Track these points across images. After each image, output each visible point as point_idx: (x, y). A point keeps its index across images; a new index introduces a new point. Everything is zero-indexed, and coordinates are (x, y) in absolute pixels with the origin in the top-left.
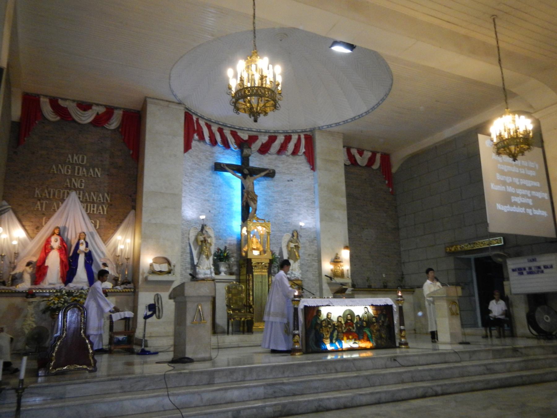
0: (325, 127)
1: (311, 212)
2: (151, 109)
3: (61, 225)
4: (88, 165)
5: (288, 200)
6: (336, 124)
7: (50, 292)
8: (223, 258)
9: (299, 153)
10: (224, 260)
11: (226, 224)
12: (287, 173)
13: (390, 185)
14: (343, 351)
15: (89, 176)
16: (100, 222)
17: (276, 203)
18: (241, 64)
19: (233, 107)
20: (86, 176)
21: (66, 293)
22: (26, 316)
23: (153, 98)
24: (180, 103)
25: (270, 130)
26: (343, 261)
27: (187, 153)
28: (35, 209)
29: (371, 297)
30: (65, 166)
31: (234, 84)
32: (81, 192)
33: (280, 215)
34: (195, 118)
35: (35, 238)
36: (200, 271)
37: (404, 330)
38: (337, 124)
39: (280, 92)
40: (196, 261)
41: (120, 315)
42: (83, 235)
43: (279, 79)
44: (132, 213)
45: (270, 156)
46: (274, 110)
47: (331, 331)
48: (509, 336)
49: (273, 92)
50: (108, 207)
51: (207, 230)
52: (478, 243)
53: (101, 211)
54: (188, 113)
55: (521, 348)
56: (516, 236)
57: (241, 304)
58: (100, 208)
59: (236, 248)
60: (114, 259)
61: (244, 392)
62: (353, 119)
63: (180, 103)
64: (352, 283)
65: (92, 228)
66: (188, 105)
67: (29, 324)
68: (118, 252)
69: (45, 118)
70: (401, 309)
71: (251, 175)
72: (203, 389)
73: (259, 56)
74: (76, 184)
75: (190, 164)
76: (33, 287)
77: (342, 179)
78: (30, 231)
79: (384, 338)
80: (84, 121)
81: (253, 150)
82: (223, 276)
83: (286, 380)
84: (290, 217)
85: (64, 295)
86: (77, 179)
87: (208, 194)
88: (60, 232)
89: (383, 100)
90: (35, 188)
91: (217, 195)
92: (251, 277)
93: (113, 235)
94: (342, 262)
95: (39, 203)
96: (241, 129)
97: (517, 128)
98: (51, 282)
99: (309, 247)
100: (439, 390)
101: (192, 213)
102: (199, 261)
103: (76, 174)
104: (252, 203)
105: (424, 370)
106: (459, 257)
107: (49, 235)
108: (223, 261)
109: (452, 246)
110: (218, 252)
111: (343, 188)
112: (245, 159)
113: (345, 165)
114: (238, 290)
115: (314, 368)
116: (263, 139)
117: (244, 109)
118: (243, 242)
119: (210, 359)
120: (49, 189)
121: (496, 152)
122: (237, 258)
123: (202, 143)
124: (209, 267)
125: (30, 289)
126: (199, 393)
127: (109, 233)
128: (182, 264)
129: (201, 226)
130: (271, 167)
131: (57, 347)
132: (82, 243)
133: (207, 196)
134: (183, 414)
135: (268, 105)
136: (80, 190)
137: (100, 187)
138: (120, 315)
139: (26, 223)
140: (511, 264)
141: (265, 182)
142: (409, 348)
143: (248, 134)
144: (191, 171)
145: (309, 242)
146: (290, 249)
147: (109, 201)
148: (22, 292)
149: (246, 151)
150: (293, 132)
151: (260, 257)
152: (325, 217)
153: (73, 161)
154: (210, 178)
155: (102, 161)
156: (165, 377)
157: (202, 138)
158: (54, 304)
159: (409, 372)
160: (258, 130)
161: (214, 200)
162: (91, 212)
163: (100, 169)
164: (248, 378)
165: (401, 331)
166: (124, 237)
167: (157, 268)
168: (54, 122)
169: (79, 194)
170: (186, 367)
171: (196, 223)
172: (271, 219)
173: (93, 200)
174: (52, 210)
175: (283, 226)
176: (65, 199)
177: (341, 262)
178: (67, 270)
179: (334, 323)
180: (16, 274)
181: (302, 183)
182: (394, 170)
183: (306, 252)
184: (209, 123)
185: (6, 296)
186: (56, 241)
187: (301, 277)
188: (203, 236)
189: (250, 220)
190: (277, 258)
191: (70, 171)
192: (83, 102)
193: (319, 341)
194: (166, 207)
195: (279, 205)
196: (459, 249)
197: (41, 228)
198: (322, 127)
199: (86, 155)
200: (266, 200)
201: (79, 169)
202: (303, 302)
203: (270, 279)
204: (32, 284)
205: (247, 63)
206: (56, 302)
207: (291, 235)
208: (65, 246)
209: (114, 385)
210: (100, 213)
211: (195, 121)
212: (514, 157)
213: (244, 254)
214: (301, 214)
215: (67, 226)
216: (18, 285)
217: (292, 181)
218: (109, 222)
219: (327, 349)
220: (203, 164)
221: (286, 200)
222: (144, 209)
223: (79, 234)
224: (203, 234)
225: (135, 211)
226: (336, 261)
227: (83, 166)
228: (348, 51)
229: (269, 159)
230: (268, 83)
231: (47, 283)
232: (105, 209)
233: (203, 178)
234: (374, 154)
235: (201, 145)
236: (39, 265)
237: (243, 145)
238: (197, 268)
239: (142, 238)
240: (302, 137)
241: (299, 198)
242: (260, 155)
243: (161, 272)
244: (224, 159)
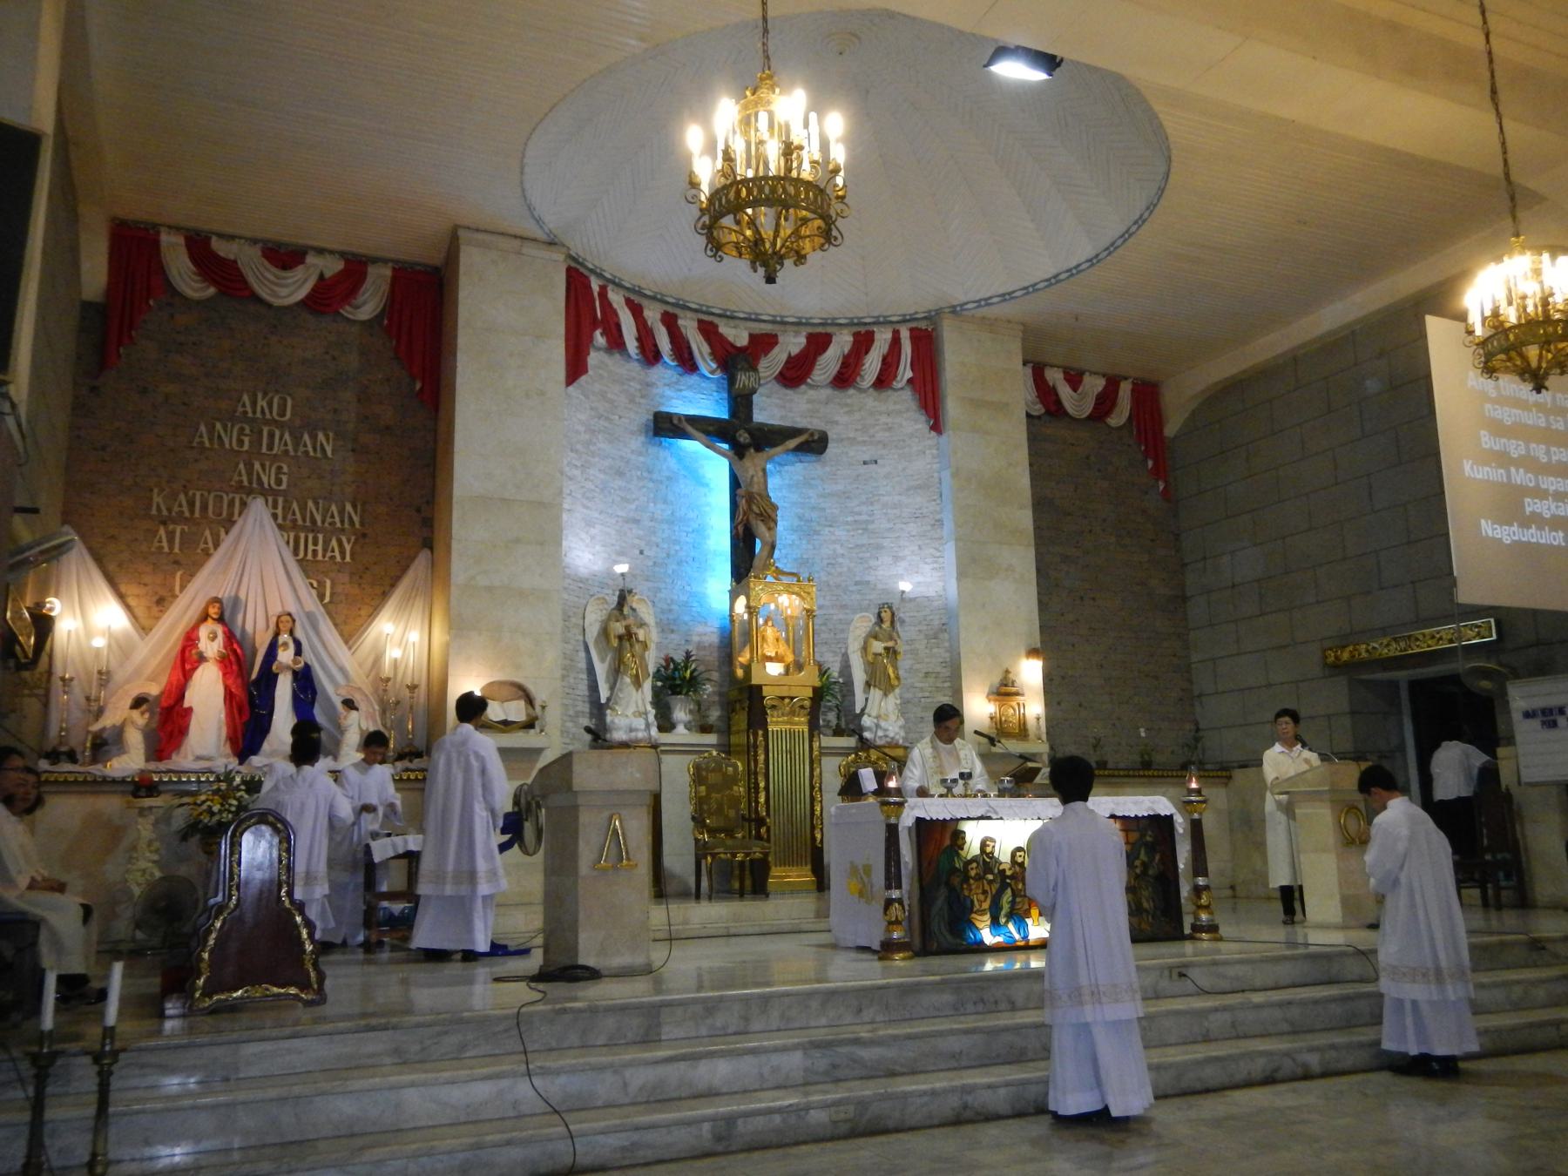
0: (969, 306)
1: (932, 551)
2: (471, 259)
3: (225, 593)
4: (298, 422)
5: (864, 517)
6: (1003, 295)
7: (198, 782)
8: (679, 685)
9: (894, 383)
10: (684, 691)
11: (688, 588)
12: (860, 439)
13: (1158, 472)
14: (1028, 948)
15: (299, 454)
16: (332, 588)
17: (831, 526)
18: (726, 110)
19: (703, 240)
20: (292, 453)
21: (244, 782)
22: (134, 848)
23: (477, 230)
24: (552, 244)
25: (811, 318)
26: (1026, 692)
27: (575, 384)
28: (153, 549)
29: (1108, 795)
30: (233, 426)
31: (706, 172)
32: (280, 500)
33: (840, 560)
34: (595, 285)
35: (154, 631)
36: (616, 721)
37: (1207, 888)
38: (1006, 297)
39: (840, 193)
40: (604, 694)
41: (394, 846)
42: (288, 622)
43: (839, 155)
44: (423, 558)
45: (811, 393)
46: (827, 246)
47: (994, 891)
48: (1514, 907)
49: (821, 191)
50: (355, 543)
51: (634, 606)
52: (1421, 637)
53: (337, 554)
54: (577, 270)
55: (1553, 940)
56: (1534, 613)
57: (732, 813)
58: (334, 543)
59: (716, 654)
60: (376, 691)
61: (748, 1065)
62: (1053, 280)
64: (1049, 756)
65: (311, 603)
66: (577, 249)
67: (144, 871)
68: (387, 670)
69: (175, 293)
70: (1196, 828)
71: (759, 449)
72: (628, 1057)
73: (778, 86)
74: (265, 479)
75: (583, 417)
76: (152, 766)
77: (1023, 455)
78: (140, 612)
79: (1146, 911)
80: (285, 297)
81: (761, 375)
82: (681, 735)
83: (869, 1032)
84: (871, 567)
85: (237, 789)
86: (267, 464)
87: (637, 503)
88: (223, 613)
89: (1140, 222)
90: (151, 490)
91: (663, 507)
92: (761, 738)
93: (374, 619)
94: (1023, 695)
95: (162, 532)
96: (729, 317)
97: (1547, 293)
98: (199, 752)
99: (927, 651)
100: (1314, 1061)
101: (591, 557)
102: (612, 694)
103: (264, 450)
104: (761, 528)
105: (1271, 1005)
106: (1365, 677)
107: (193, 622)
108: (680, 693)
109: (1344, 647)
110: (666, 668)
111: (1025, 481)
112: (741, 403)
113: (1028, 415)
114: (724, 775)
115: (948, 998)
116: (793, 343)
117: (737, 246)
118: (737, 639)
119: (648, 970)
120: (191, 493)
121: (1482, 365)
122: (721, 686)
123: (617, 356)
124: (642, 709)
125: (142, 771)
126: (617, 1069)
127: (360, 616)
128: (565, 701)
129: (617, 593)
130: (815, 424)
131: (214, 935)
132: (285, 644)
133: (633, 507)
134: (571, 1127)
135: (804, 231)
136: (275, 493)
137: (333, 485)
138: (394, 846)
139: (129, 589)
140: (1521, 697)
141: (799, 466)
142: (1221, 939)
143: (746, 329)
144: (587, 437)
145: (927, 637)
146: (870, 658)
147: (357, 526)
148: (123, 781)
149: (743, 379)
150: (876, 323)
151: (787, 680)
152: (971, 566)
153: (254, 412)
154: (642, 459)
155: (335, 411)
156: (519, 1021)
158: (212, 814)
159: (1225, 1009)
160: (778, 319)
162: (310, 556)
163: (331, 435)
164: (756, 1025)
165: (1197, 891)
166: (402, 625)
168: (199, 302)
169: (275, 506)
170: (580, 994)
171: (603, 585)
172: (818, 572)
173: (314, 521)
174: (199, 551)
175: (852, 591)
176: (236, 517)
177: (1017, 694)
178: (245, 719)
179: (1001, 868)
180: (104, 729)
181: (904, 469)
182: (1171, 429)
183: (918, 666)
184: (632, 297)
185: (80, 793)
186: (214, 638)
187: (905, 739)
188: (624, 623)
189: (755, 577)
190: (835, 683)
191: (246, 440)
192: (280, 245)
193: (960, 919)
194: (517, 541)
195: (840, 533)
196: (1364, 655)
197: (171, 603)
198: (962, 305)
199: (290, 395)
200: (800, 518)
201: (271, 436)
202: (912, 809)
203: (816, 745)
204: (148, 760)
205: (745, 107)
206: (216, 808)
207: (873, 619)
208: (239, 651)
209: (375, 1044)
210: (333, 557)
211: (596, 294)
212: (1538, 381)
213: (740, 673)
214: (903, 558)
215: (242, 596)
216: (110, 760)
217: (876, 462)
218: (360, 584)
219: (982, 942)
220: (620, 417)
221: (857, 518)
222: (455, 546)
223: (274, 619)
224: (625, 618)
225: (432, 552)
226: (1004, 691)
227: (281, 426)
228: (1037, 76)
229: (809, 401)
230: (806, 166)
231: (191, 758)
232: (348, 548)
233: (622, 457)
234: (1113, 383)
235: (613, 363)
236: (165, 705)
237: (733, 360)
238: (608, 712)
239: (450, 628)
240: (905, 335)
241: (897, 512)
244: (680, 402)
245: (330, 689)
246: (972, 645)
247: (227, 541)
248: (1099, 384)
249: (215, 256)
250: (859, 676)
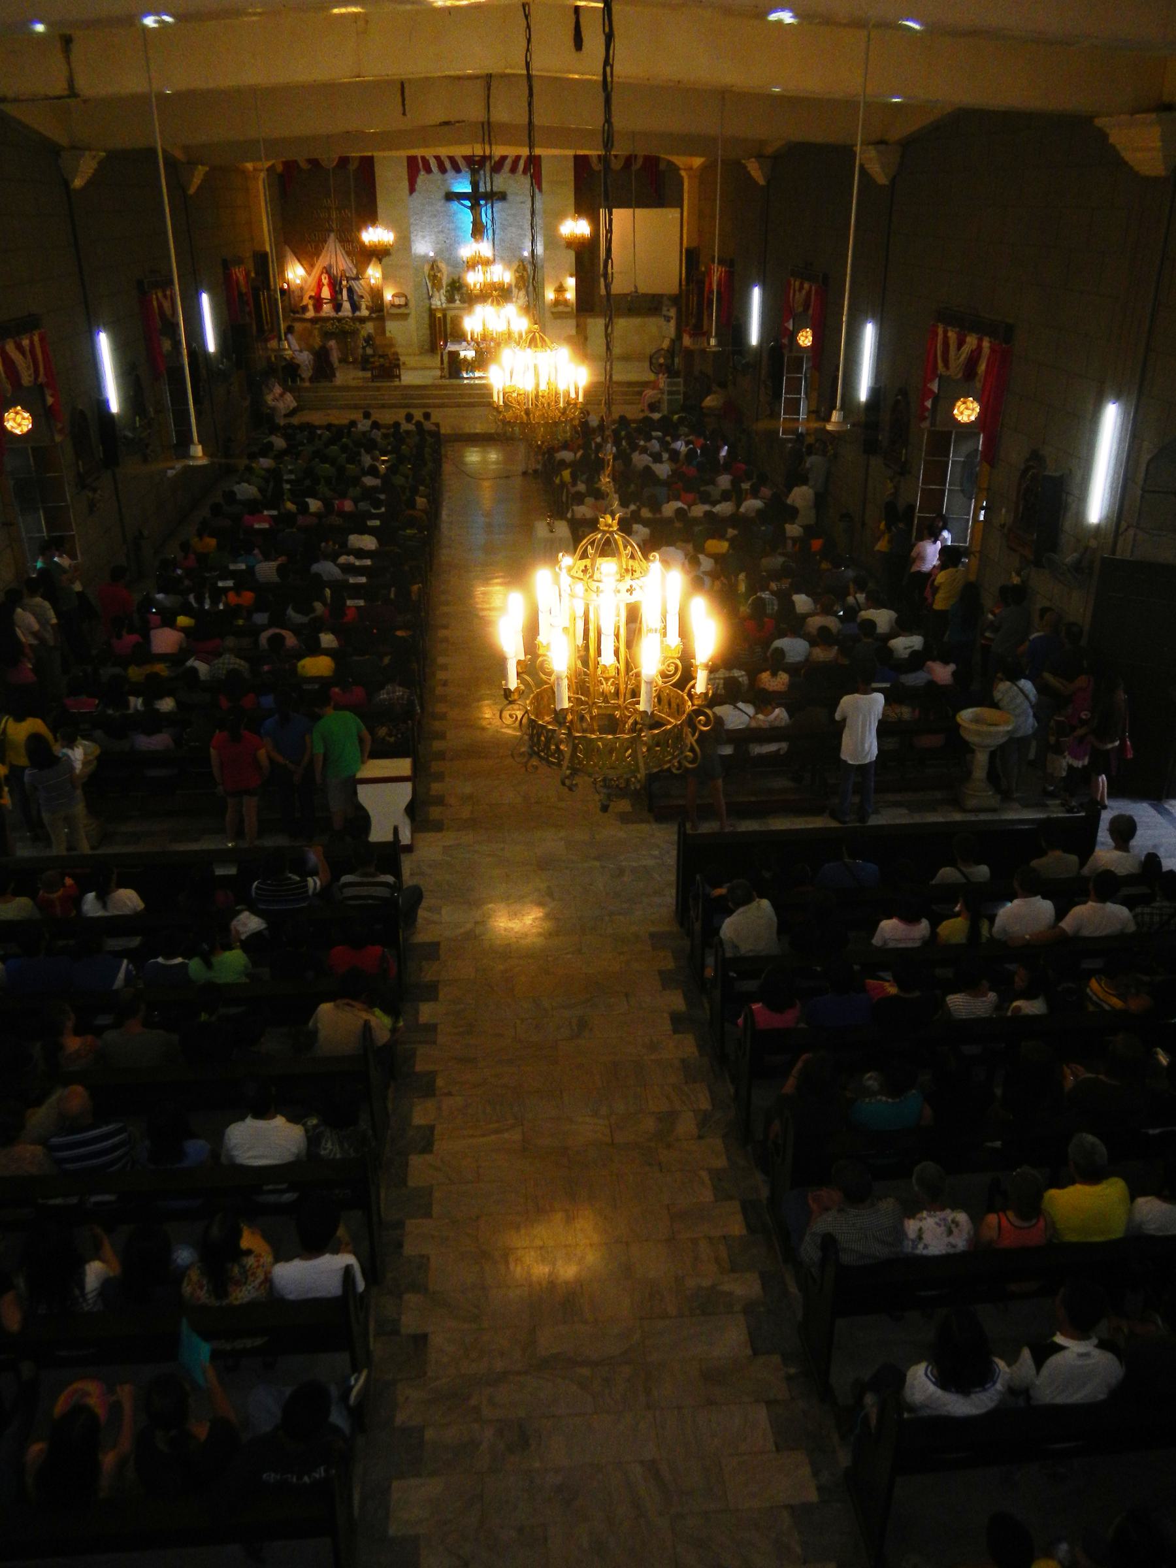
3: (326, 264)
45: (504, 176)
88: (327, 270)
139: (304, 262)
157: (429, 170)
161: (449, 229)
167: (397, 301)
226: (560, 289)
235: (431, 176)
237: (475, 165)
243: (399, 306)
245: (358, 290)
246: (548, 272)
247: (326, 246)
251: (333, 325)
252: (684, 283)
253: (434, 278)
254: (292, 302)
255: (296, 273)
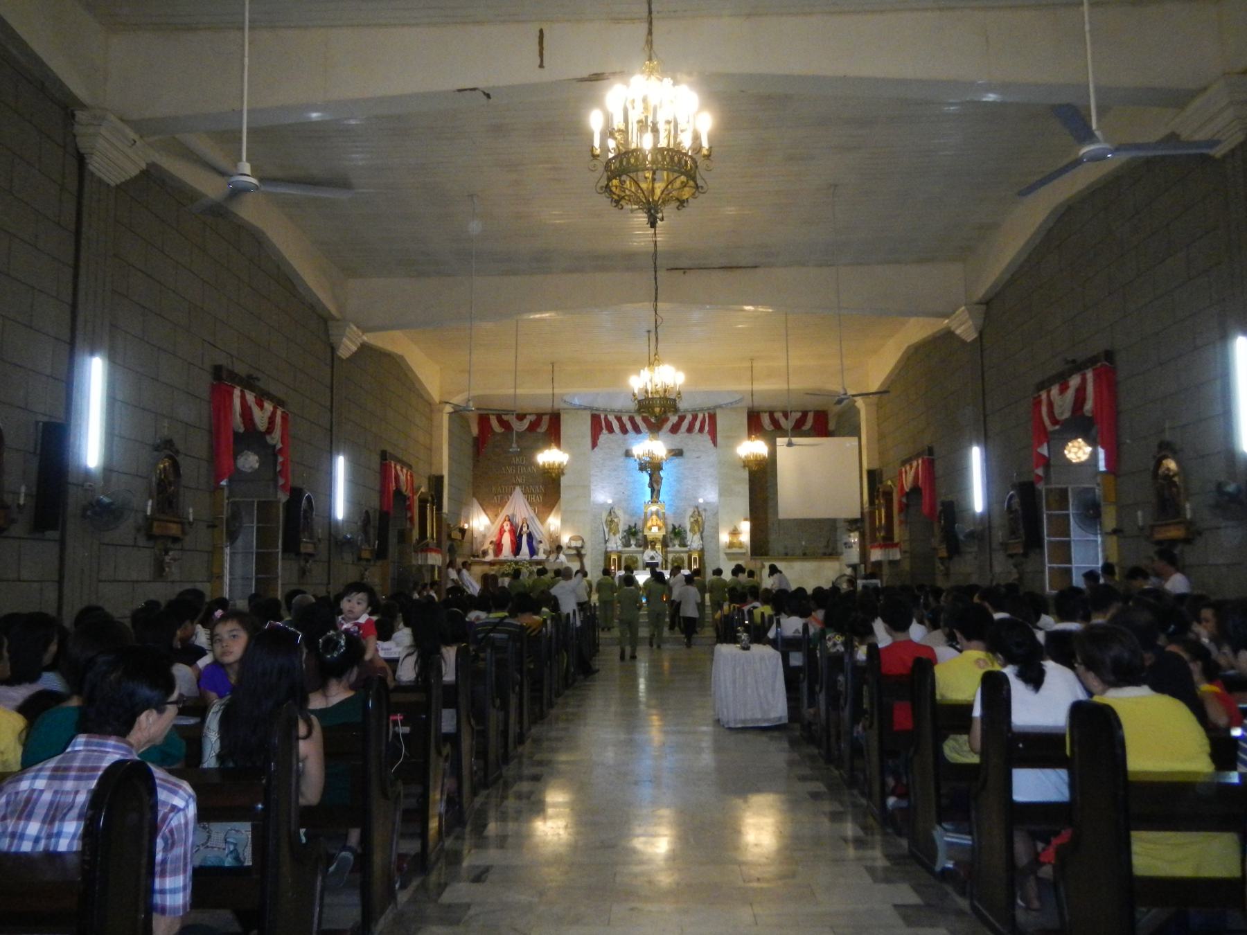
2: (564, 418)
3: (510, 513)
34: (602, 417)
54: (595, 414)
63: (585, 408)
65: (532, 514)
66: (596, 405)
69: (495, 432)
82: (633, 548)
88: (510, 519)
95: (495, 498)
98: (505, 555)
104: (655, 486)
114: (633, 561)
118: (648, 517)
123: (614, 433)
139: (488, 512)
157: (611, 430)
167: (574, 544)
184: (619, 414)
226: (735, 532)
232: (541, 498)
235: (611, 436)
240: (707, 415)
242: (672, 435)
245: (537, 536)
247: (511, 498)
248: (799, 415)
249: (502, 419)
250: (688, 527)
251: (510, 566)
252: (866, 505)
253: (610, 523)
254: (474, 546)
255: (480, 523)
